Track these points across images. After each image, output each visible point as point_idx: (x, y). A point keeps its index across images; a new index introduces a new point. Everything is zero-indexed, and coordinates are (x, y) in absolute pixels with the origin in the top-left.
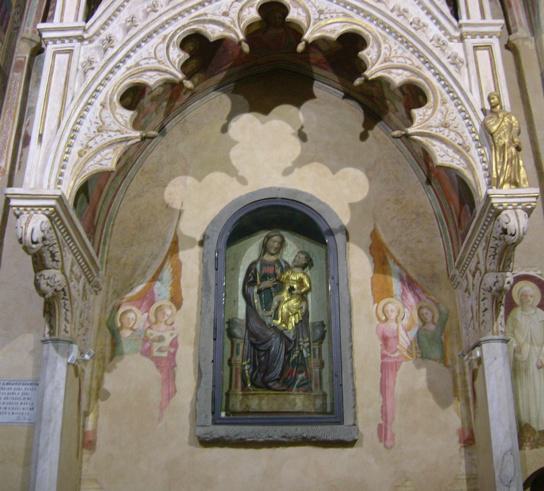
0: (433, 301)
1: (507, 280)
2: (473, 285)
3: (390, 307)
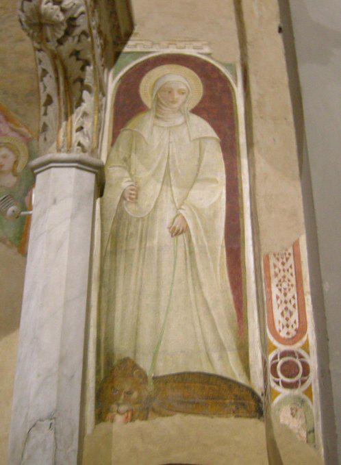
0: (22, 135)
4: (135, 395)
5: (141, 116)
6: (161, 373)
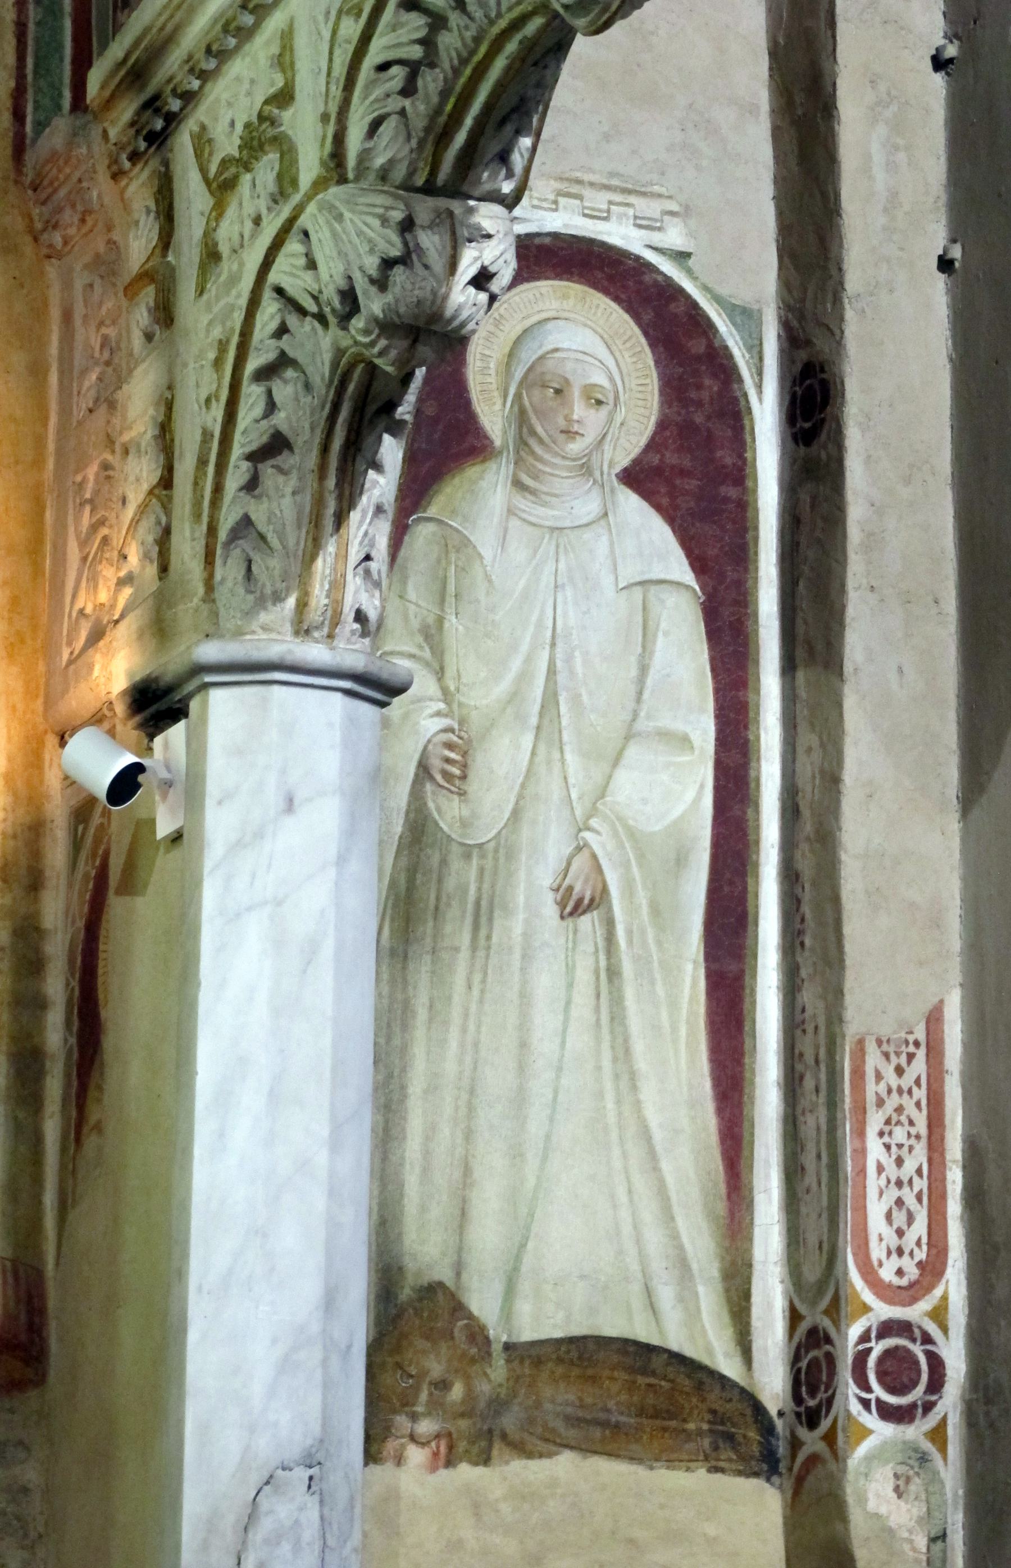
1: (468, 266)
2: (211, 256)
4: (457, 1392)
5: (472, 472)
6: (527, 1334)
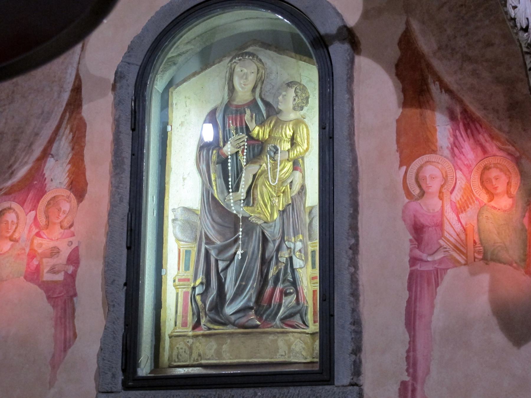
3: (430, 170)
